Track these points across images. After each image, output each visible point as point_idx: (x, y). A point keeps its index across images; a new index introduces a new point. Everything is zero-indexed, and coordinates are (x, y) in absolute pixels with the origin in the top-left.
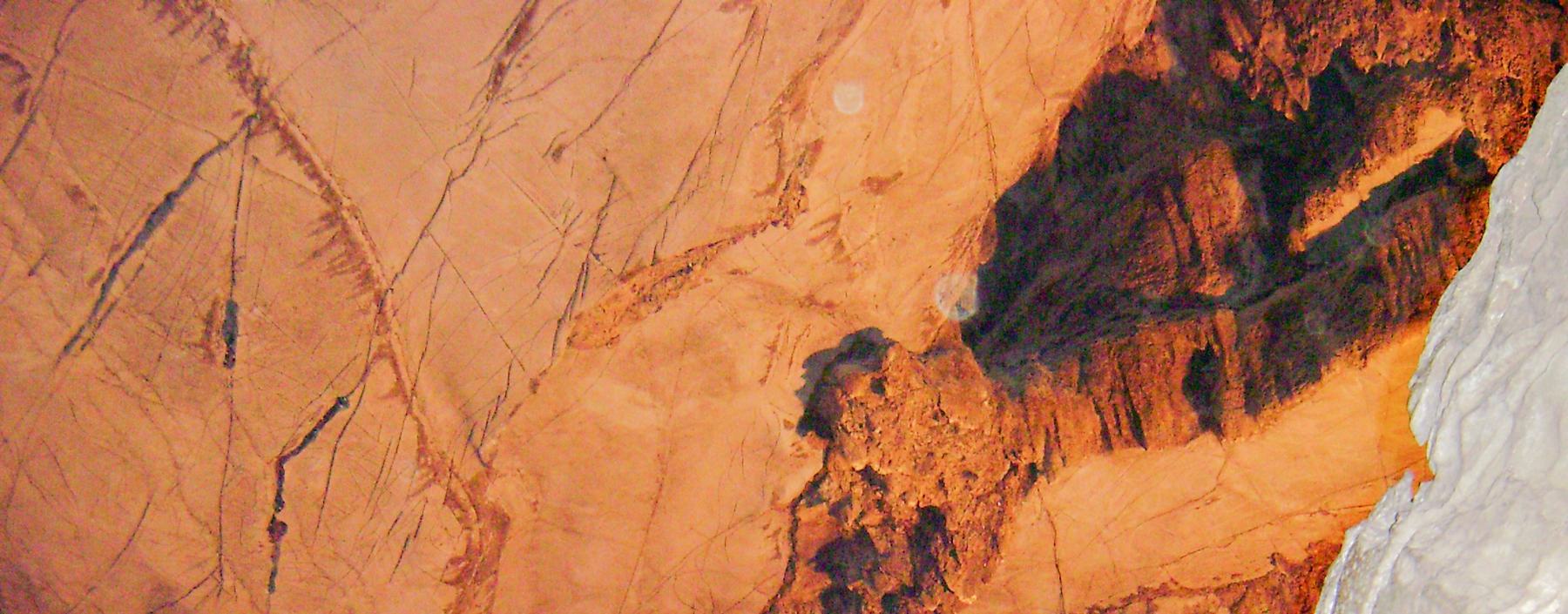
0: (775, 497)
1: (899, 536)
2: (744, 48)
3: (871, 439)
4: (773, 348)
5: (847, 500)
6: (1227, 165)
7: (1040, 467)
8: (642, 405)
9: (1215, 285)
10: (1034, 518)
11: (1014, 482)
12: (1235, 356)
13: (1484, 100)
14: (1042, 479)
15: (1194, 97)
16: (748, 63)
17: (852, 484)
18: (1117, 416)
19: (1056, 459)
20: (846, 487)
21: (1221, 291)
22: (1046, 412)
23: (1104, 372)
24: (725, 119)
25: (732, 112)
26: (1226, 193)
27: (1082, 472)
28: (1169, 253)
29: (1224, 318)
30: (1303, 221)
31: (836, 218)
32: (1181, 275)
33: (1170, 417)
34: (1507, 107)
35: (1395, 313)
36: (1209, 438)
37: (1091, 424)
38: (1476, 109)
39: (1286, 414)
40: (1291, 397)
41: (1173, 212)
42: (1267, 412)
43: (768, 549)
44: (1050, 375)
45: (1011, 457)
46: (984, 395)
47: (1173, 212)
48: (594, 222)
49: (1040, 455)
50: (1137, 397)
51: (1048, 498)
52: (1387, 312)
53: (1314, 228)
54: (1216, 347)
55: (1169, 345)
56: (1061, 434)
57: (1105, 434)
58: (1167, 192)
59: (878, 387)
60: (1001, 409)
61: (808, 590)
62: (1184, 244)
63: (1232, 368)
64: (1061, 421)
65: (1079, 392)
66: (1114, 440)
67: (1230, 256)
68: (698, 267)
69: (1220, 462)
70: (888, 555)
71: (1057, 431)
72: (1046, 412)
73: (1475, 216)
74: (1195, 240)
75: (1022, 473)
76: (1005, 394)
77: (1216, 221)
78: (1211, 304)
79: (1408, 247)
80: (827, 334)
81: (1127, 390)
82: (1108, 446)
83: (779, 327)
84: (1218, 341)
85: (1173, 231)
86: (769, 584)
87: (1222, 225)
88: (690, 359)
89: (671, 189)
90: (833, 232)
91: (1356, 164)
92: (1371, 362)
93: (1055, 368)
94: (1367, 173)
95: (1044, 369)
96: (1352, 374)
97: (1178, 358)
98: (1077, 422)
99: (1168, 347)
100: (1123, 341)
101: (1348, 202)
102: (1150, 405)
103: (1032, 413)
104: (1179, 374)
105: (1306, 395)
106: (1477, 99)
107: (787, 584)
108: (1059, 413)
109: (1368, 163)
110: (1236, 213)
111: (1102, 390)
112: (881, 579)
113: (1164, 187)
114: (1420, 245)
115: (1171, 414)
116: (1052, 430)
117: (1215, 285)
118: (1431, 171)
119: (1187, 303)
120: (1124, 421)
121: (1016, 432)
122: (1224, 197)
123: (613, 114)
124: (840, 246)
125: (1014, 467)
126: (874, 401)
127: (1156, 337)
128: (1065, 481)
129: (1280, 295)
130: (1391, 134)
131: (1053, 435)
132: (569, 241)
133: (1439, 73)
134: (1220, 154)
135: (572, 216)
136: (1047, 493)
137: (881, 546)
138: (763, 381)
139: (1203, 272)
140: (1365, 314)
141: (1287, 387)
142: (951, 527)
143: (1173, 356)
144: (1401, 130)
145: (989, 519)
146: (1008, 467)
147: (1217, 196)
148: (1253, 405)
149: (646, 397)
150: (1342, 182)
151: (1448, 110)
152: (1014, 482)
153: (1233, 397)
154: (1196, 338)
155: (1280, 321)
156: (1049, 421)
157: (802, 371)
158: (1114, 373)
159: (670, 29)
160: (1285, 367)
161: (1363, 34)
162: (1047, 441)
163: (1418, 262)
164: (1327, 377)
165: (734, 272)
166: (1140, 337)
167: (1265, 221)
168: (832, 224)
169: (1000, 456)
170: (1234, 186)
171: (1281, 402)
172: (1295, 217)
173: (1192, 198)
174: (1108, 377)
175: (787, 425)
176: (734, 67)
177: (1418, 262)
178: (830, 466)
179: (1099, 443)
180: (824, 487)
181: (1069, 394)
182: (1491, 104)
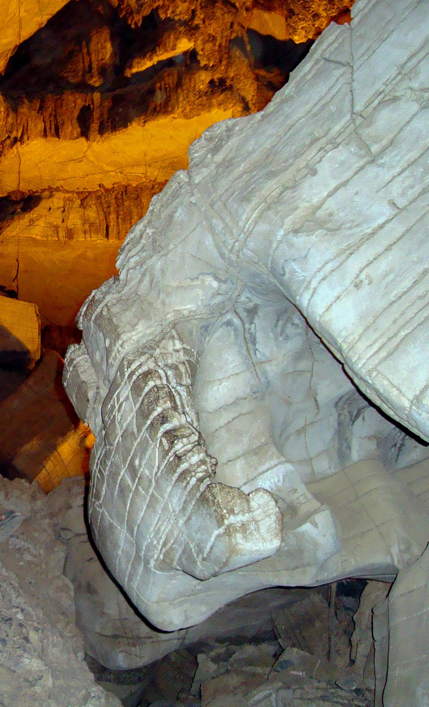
6: (108, 37)
7: (19, 139)
9: (96, 82)
10: (13, 156)
11: (8, 142)
12: (98, 110)
13: (202, 40)
14: (19, 143)
15: (100, 8)
18: (51, 124)
19: (25, 137)
21: (97, 85)
22: (25, 118)
23: (49, 107)
27: (34, 142)
28: (81, 66)
29: (97, 96)
30: (131, 67)
32: (84, 76)
33: (70, 128)
34: (211, 44)
36: (83, 139)
37: (41, 126)
38: (199, 42)
39: (113, 137)
40: (115, 131)
42: (106, 135)
44: (28, 103)
45: (9, 133)
46: (2, 109)
47: (85, 51)
50: (59, 119)
51: (20, 149)
52: (155, 109)
53: (135, 70)
54: (92, 106)
55: (75, 102)
56: (29, 128)
58: (84, 43)
60: (8, 115)
62: (87, 64)
63: (96, 115)
64: (29, 123)
65: (38, 113)
66: (48, 133)
67: (102, 71)
69: (85, 149)
71: (27, 126)
72: (25, 118)
75: (12, 139)
76: (10, 110)
77: (100, 58)
78: (93, 89)
79: (167, 86)
81: (55, 116)
82: (45, 135)
84: (93, 103)
85: (83, 58)
87: (102, 59)
91: (153, 51)
92: (146, 125)
93: (30, 101)
94: (157, 56)
95: (26, 101)
96: (140, 128)
97: (77, 107)
99: (75, 102)
100: (58, 97)
101: (148, 64)
102: (63, 124)
103: (19, 118)
104: (76, 114)
105: (121, 132)
106: (200, 38)
108: (29, 119)
109: (158, 53)
110: (108, 56)
111: (47, 115)
113: (83, 39)
114: (171, 86)
115: (71, 127)
116: (26, 125)
117: (96, 82)
119: (83, 87)
120: (53, 127)
121: (12, 124)
122: (103, 49)
125: (9, 137)
127: (70, 97)
128: (28, 144)
129: (118, 92)
130: (167, 44)
131: (25, 128)
133: (188, 26)
134: (106, 33)
136: (19, 148)
139: (92, 76)
140: (148, 107)
141: (114, 129)
143: (75, 106)
144: (171, 44)
146: (7, 135)
147: (102, 48)
148: (101, 132)
150: (148, 56)
151: (190, 40)
152: (8, 142)
153: (95, 126)
154: (85, 101)
155: (117, 101)
158: (52, 108)
160: (115, 120)
162: (23, 130)
163: (170, 93)
164: (130, 127)
166: (65, 96)
167: (118, 62)
169: (4, 131)
170: (109, 45)
171: (112, 132)
172: (128, 64)
173: (92, 47)
174: (50, 109)
177: (170, 93)
179: (43, 133)
181: (34, 113)
182: (205, 42)
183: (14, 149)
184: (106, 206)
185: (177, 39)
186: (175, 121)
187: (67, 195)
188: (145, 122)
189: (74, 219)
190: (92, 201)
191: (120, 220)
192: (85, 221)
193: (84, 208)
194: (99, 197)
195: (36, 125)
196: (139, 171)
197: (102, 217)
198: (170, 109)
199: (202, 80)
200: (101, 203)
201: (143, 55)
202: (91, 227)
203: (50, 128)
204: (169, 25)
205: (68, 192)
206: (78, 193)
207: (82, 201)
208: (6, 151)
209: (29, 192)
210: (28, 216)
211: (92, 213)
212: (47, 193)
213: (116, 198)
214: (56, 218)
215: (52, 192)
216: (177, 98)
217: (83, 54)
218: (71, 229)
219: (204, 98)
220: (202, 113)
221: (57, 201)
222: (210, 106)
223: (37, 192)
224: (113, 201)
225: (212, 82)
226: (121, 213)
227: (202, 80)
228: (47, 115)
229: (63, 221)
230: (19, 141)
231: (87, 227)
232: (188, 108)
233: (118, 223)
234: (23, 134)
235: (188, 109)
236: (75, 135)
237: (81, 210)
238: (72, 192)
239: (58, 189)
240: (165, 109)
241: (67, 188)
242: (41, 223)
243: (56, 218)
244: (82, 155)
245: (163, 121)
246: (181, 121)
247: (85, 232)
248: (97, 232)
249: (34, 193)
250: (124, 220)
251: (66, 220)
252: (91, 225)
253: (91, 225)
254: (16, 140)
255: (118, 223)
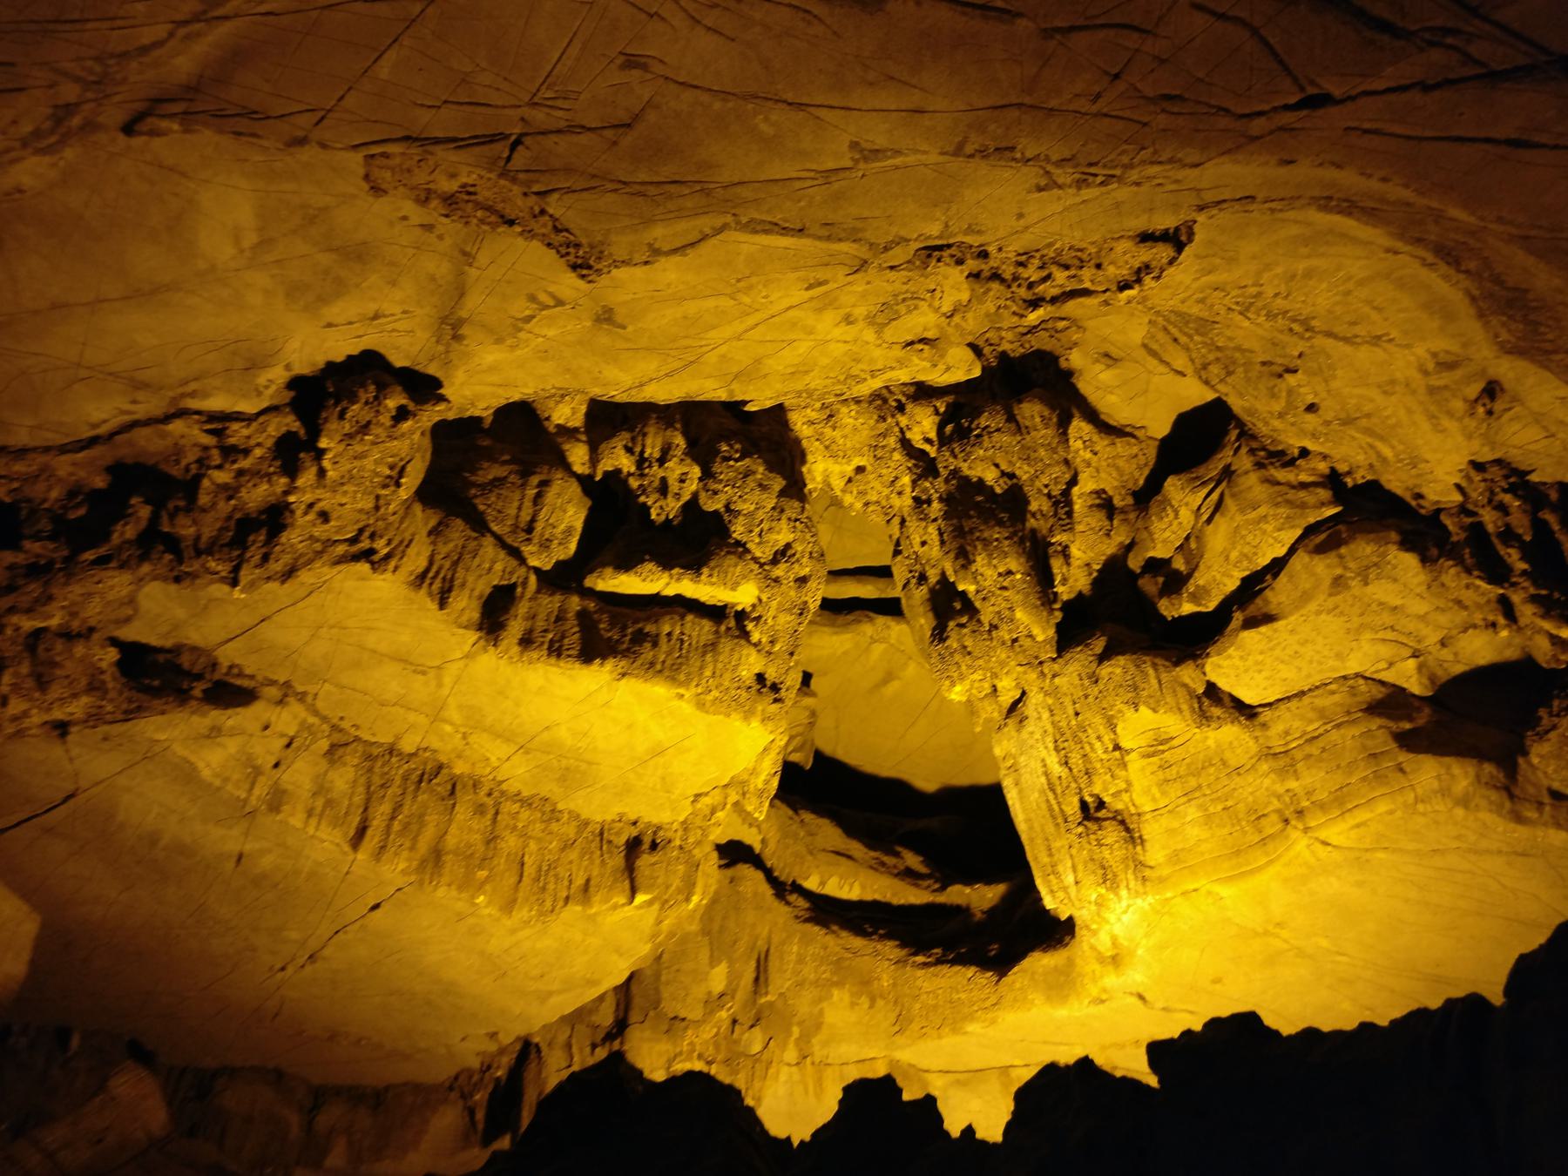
0: (183, 395)
1: (224, 507)
2: (812, 174)
3: (350, 436)
4: (376, 317)
5: (246, 452)
8: (237, 240)
11: (341, 549)
14: (364, 567)
16: (798, 185)
17: (259, 445)
19: (393, 563)
20: (252, 442)
24: (738, 190)
25: (745, 192)
26: (565, 511)
27: (380, 583)
31: (560, 303)
35: (659, 667)
41: (531, 492)
42: (535, 655)
43: (97, 416)
48: (563, 124)
49: (385, 551)
50: (460, 574)
52: (652, 664)
54: (519, 590)
55: (494, 562)
57: (422, 577)
58: (535, 480)
59: (402, 414)
61: (71, 469)
62: (525, 516)
63: (522, 608)
68: (518, 229)
70: (204, 510)
72: (411, 531)
73: (736, 656)
74: (533, 520)
80: (404, 347)
81: (455, 563)
83: (404, 312)
86: (49, 435)
88: (325, 259)
89: (643, 176)
90: (547, 307)
92: (624, 681)
98: (418, 554)
107: (63, 449)
111: (444, 549)
112: (182, 520)
115: (466, 604)
118: (716, 613)
122: (566, 516)
123: (705, 98)
124: (529, 319)
125: (353, 541)
126: (385, 419)
132: (526, 112)
135: (559, 103)
137: (204, 499)
138: (330, 325)
142: (284, 537)
145: (301, 555)
148: (526, 642)
149: (250, 239)
153: (515, 628)
156: (407, 536)
157: (355, 351)
159: (823, 113)
161: (750, 514)
165: (465, 254)
168: (552, 303)
174: (451, 545)
175: (288, 367)
176: (795, 175)
178: (261, 419)
180: (235, 426)
183: (339, 568)
184: (377, 781)
185: (744, 577)
186: (676, 703)
187: (312, 720)
188: (624, 675)
189: (301, 774)
190: (352, 758)
191: (396, 826)
192: (320, 789)
193: (332, 762)
194: (369, 757)
195: (418, 554)
196: (495, 751)
197: (358, 799)
198: (682, 677)
199: (751, 663)
200: (370, 770)
201: (666, 564)
202: (324, 805)
203: (435, 577)
204: (740, 549)
205: (316, 713)
206: (334, 728)
207: (333, 747)
208: (318, 564)
209: (231, 667)
210: (216, 716)
211: (343, 779)
212: (273, 692)
213: (405, 778)
214: (266, 750)
215: (286, 695)
216: (702, 668)
217: (523, 497)
218: (284, 792)
219: (745, 694)
220: (734, 715)
221: (287, 719)
222: (748, 715)
223: (252, 677)
224: (398, 781)
225: (760, 678)
226: (406, 810)
227: (751, 663)
228: (444, 549)
229: (276, 765)
230: (372, 563)
231: (320, 803)
232: (715, 693)
233: (389, 827)
234: (388, 557)
235: (710, 697)
236: (464, 619)
237: (323, 764)
238: (325, 719)
239: (302, 697)
240: (671, 671)
241: (320, 704)
242: (232, 746)
243: (266, 750)
244: (437, 663)
245: (659, 690)
246: (687, 708)
247: (310, 813)
248: (335, 824)
249: (241, 675)
250: (406, 826)
251: (282, 767)
252: (329, 803)
253: (329, 803)
254: (367, 555)
255: (389, 827)
